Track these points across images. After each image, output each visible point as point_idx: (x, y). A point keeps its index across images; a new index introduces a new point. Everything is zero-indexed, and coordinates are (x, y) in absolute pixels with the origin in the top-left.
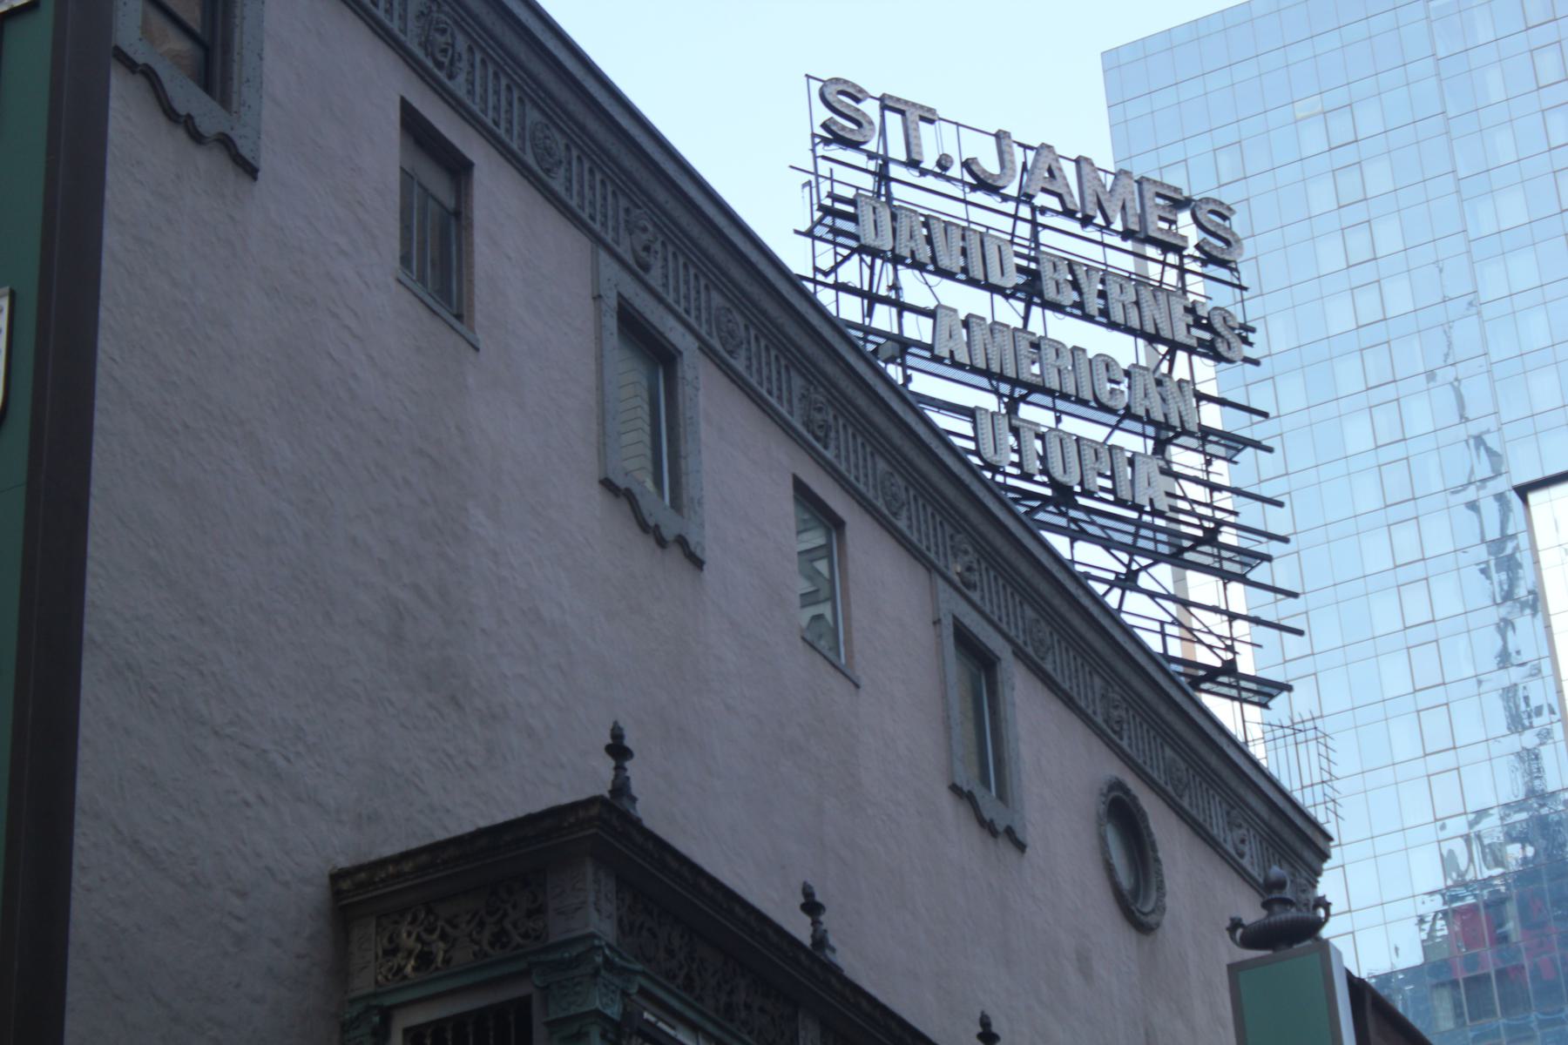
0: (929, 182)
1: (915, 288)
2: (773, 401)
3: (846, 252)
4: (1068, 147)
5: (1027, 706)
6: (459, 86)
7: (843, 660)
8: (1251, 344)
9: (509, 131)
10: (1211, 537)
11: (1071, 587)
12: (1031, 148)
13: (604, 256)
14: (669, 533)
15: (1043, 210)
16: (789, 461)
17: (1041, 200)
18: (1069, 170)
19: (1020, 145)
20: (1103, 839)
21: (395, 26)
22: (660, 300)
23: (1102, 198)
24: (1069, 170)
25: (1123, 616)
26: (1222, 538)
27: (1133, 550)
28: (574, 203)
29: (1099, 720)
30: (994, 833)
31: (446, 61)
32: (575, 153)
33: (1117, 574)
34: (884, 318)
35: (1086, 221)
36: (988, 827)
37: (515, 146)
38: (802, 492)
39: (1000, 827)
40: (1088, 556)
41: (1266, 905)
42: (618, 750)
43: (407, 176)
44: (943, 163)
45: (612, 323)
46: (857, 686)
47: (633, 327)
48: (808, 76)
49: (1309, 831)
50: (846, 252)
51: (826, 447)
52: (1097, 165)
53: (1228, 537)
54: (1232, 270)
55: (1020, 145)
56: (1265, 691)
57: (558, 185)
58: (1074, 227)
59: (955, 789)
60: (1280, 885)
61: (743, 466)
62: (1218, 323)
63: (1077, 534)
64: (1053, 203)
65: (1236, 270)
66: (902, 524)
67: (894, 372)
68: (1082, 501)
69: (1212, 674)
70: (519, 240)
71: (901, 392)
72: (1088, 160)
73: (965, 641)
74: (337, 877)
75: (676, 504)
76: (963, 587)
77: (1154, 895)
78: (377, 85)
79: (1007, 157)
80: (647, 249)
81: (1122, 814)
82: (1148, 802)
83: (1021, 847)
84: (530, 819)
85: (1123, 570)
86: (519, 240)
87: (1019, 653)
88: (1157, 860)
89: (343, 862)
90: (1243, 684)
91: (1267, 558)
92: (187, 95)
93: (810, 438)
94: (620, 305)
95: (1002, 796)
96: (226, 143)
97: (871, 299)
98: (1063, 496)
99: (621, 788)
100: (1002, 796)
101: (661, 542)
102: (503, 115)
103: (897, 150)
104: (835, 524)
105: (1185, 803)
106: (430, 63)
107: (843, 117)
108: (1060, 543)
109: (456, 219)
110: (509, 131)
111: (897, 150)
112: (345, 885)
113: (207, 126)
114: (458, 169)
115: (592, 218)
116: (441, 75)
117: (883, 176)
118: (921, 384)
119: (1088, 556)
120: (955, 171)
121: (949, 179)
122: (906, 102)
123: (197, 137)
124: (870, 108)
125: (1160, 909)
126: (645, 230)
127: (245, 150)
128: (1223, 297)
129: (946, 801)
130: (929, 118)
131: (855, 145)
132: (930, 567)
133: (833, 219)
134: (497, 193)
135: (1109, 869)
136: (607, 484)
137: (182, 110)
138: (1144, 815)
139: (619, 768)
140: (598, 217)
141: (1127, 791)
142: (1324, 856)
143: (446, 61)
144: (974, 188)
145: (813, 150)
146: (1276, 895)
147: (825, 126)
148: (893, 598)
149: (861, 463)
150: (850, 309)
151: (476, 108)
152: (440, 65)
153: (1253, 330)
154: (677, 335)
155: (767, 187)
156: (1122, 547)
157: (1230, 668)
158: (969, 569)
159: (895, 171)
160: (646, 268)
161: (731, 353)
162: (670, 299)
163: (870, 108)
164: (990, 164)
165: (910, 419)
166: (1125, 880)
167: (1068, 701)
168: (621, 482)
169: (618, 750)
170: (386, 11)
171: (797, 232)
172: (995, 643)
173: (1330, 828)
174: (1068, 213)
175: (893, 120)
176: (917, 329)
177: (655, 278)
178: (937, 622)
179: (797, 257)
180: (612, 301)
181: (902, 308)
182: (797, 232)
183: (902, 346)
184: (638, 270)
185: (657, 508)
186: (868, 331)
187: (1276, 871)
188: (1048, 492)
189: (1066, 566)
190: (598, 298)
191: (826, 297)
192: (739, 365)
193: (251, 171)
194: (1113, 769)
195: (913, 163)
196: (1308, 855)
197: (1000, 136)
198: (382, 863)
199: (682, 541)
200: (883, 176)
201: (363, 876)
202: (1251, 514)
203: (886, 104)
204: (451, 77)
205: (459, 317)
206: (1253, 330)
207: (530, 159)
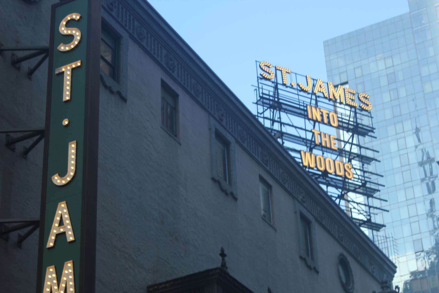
0: (288, 89)
2: (254, 154)
3: (266, 108)
5: (320, 236)
6: (175, 74)
7: (272, 223)
8: (374, 133)
9: (188, 86)
11: (327, 198)
13: (211, 118)
14: (229, 192)
15: (319, 97)
16: (257, 170)
17: (318, 94)
20: (338, 270)
21: (159, 59)
22: (225, 129)
27: (343, 189)
28: (204, 104)
29: (337, 237)
31: (172, 68)
32: (204, 91)
33: (338, 195)
34: (276, 126)
35: (330, 100)
36: (309, 267)
37: (189, 89)
38: (262, 179)
39: (312, 267)
41: (382, 288)
42: (223, 255)
43: (163, 98)
45: (214, 136)
46: (276, 230)
47: (219, 136)
49: (391, 266)
50: (266, 108)
51: (267, 166)
53: (368, 185)
57: (200, 99)
58: (327, 101)
59: (301, 257)
61: (246, 171)
63: (328, 185)
66: (286, 186)
67: (279, 140)
69: (364, 223)
70: (192, 116)
71: (282, 146)
73: (303, 217)
74: (149, 287)
75: (230, 183)
76: (302, 203)
77: (351, 285)
78: (156, 75)
80: (222, 115)
81: (343, 262)
82: (350, 259)
84: (200, 273)
85: (340, 194)
86: (192, 116)
87: (316, 220)
88: (352, 275)
89: (150, 283)
91: (379, 191)
92: (110, 82)
93: (263, 164)
96: (119, 93)
97: (273, 121)
98: (325, 173)
99: (224, 265)
100: (312, 258)
101: (227, 194)
103: (280, 81)
104: (269, 187)
105: (359, 259)
106: (168, 69)
108: (324, 187)
109: (175, 109)
110: (188, 86)
112: (151, 289)
113: (115, 89)
114: (175, 96)
115: (208, 108)
116: (171, 72)
117: (276, 88)
118: (288, 144)
121: (294, 89)
123: (112, 92)
125: (353, 288)
127: (124, 94)
129: (299, 261)
131: (269, 80)
132: (294, 197)
133: (262, 100)
134: (185, 104)
135: (340, 277)
136: (213, 179)
137: (108, 85)
138: (348, 263)
139: (223, 259)
140: (210, 107)
141: (344, 256)
142: (395, 272)
143: (172, 68)
144: (300, 91)
145: (258, 81)
146: (385, 285)
147: (261, 75)
148: (285, 206)
150: (267, 124)
151: (179, 80)
152: (170, 69)
154: (229, 138)
156: (340, 188)
157: (369, 221)
158: (304, 197)
159: (279, 87)
160: (222, 120)
161: (243, 142)
162: (228, 128)
166: (344, 281)
167: (329, 232)
168: (217, 178)
169: (223, 255)
171: (253, 103)
172: (310, 217)
173: (397, 265)
174: (325, 98)
176: (285, 129)
177: (224, 123)
178: (296, 212)
179: (253, 109)
180: (214, 130)
181: (281, 123)
182: (253, 103)
183: (282, 134)
184: (219, 121)
185: (225, 185)
186: (272, 130)
187: (385, 278)
189: (326, 193)
190: (210, 129)
191: (261, 120)
192: (245, 145)
193: (124, 100)
194: (340, 250)
195: (284, 85)
196: (391, 272)
198: (161, 284)
199: (232, 194)
200: (276, 88)
201: (156, 287)
202: (374, 178)
204: (173, 72)
205: (176, 136)
207: (193, 93)
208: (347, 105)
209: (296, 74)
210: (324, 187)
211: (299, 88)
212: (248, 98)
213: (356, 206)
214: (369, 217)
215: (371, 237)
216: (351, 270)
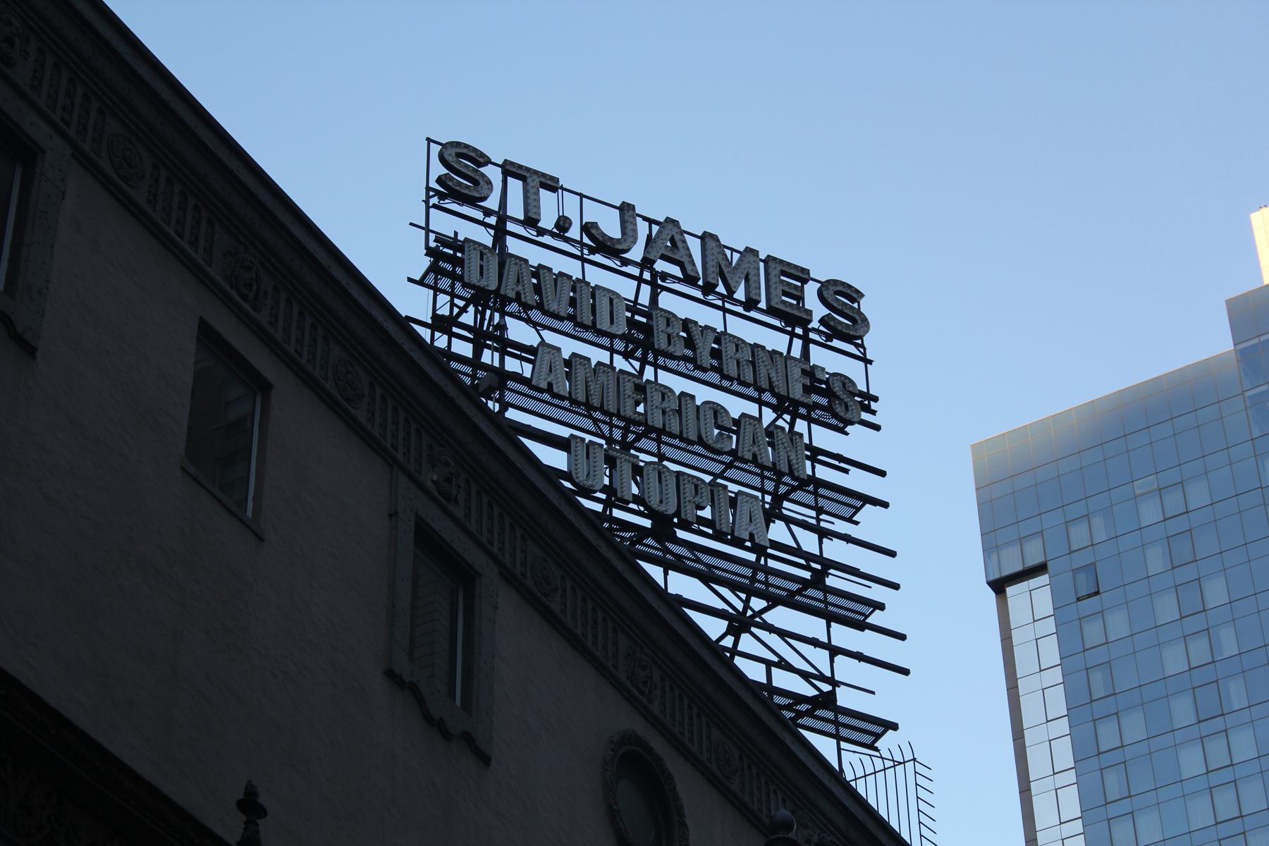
1: (518, 331)
2: (184, 244)
3: (461, 303)
4: (693, 223)
7: (249, 514)
8: (874, 412)
10: (818, 580)
12: (657, 223)
15: (665, 276)
17: (661, 266)
18: (695, 246)
19: (645, 219)
23: (725, 270)
24: (695, 246)
25: (738, 661)
26: (831, 581)
30: (446, 735)
40: (681, 585)
44: (563, 224)
46: (261, 539)
48: (429, 140)
50: (461, 303)
52: (723, 242)
54: (857, 346)
55: (645, 219)
56: (870, 730)
59: (391, 675)
60: (787, 826)
62: (837, 388)
64: (676, 271)
65: (862, 346)
68: (681, 534)
71: (498, 420)
72: (715, 238)
79: (630, 227)
82: (676, 766)
83: (485, 759)
87: (508, 576)
88: (685, 826)
90: (842, 719)
91: (881, 607)
94: (417, 524)
95: (467, 705)
97: (479, 338)
102: (496, 537)
103: (516, 208)
105: (735, 787)
107: (460, 174)
108: (656, 572)
111: (516, 208)
117: (500, 233)
119: (681, 585)
120: (574, 232)
121: (568, 240)
122: (528, 170)
124: (493, 173)
126: (447, 464)
128: (852, 369)
130: (551, 184)
131: (473, 202)
135: (613, 814)
144: (593, 251)
145: (427, 202)
149: (764, 797)
153: (876, 399)
155: (384, 243)
157: (828, 700)
163: (493, 173)
164: (611, 226)
165: (620, 566)
170: (404, 454)
171: (410, 280)
174: (690, 280)
175: (515, 186)
178: (393, 515)
179: (415, 304)
182: (410, 280)
183: (503, 376)
188: (647, 523)
197: (626, 210)
200: (500, 233)
203: (509, 170)
206: (876, 399)
208: (771, 311)
209: (582, 196)
210: (656, 572)
211: (586, 240)
212: (392, 265)
213: (778, 652)
214: (826, 688)
215: (831, 757)
216: (680, 809)
